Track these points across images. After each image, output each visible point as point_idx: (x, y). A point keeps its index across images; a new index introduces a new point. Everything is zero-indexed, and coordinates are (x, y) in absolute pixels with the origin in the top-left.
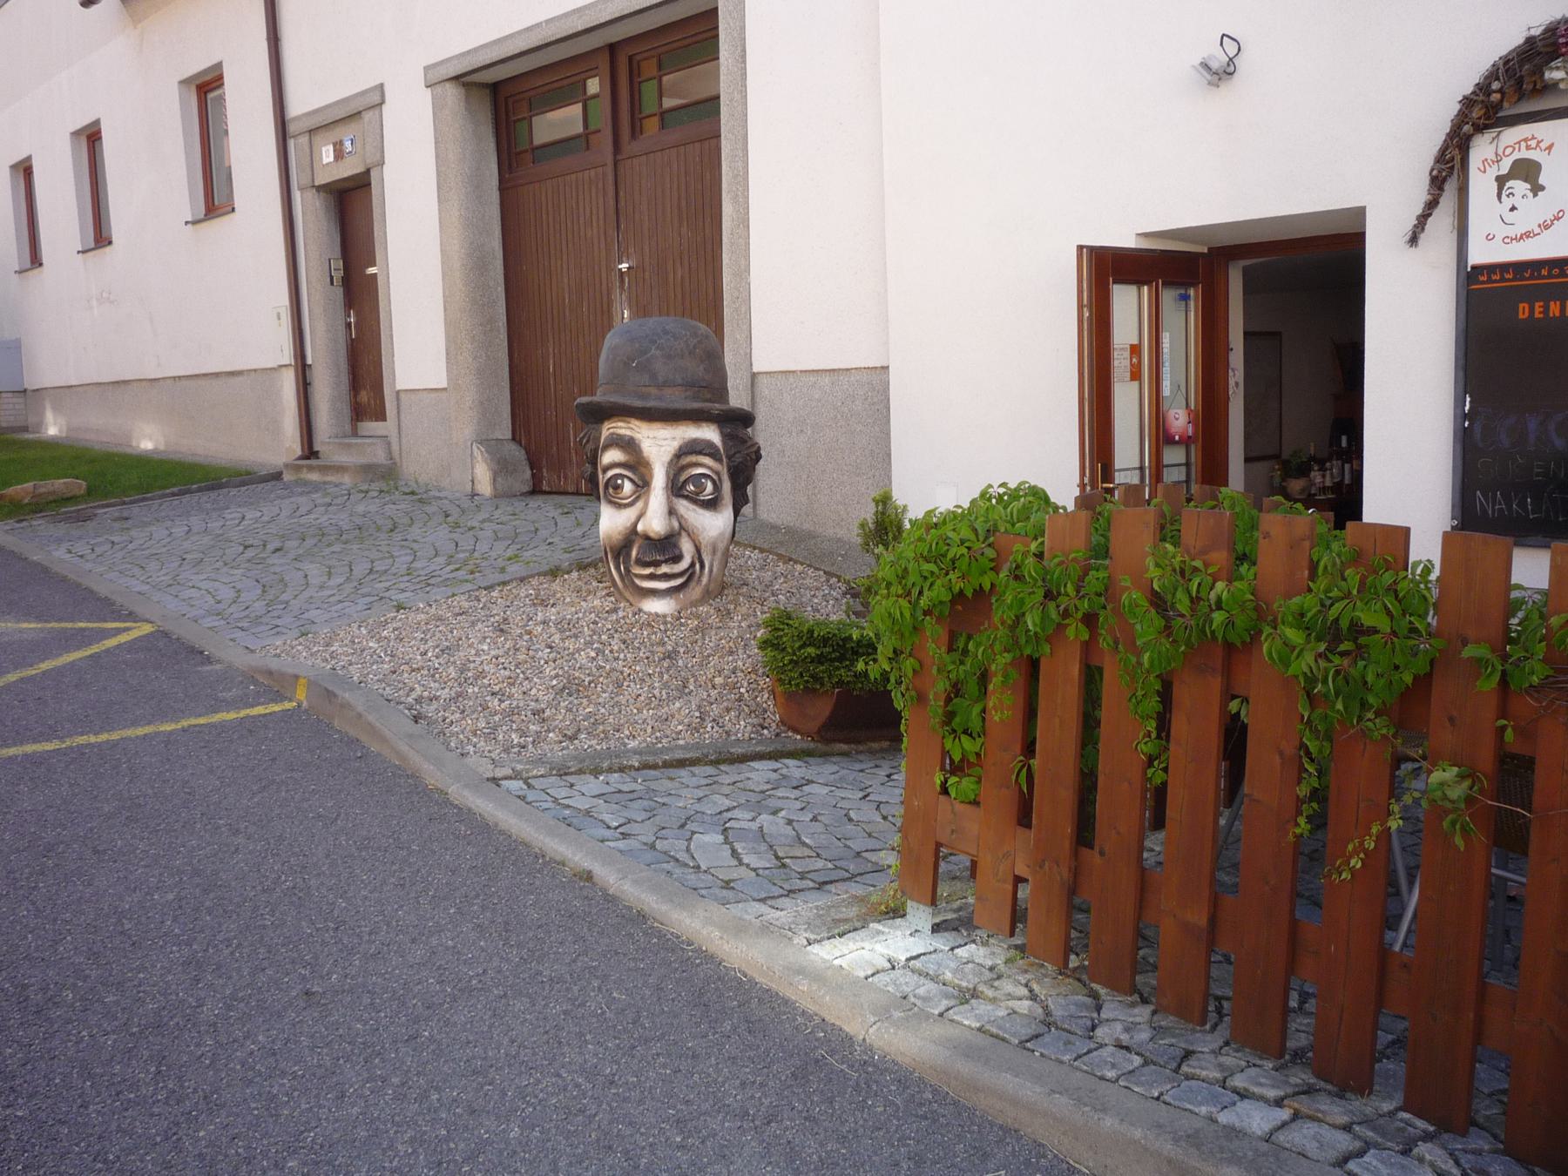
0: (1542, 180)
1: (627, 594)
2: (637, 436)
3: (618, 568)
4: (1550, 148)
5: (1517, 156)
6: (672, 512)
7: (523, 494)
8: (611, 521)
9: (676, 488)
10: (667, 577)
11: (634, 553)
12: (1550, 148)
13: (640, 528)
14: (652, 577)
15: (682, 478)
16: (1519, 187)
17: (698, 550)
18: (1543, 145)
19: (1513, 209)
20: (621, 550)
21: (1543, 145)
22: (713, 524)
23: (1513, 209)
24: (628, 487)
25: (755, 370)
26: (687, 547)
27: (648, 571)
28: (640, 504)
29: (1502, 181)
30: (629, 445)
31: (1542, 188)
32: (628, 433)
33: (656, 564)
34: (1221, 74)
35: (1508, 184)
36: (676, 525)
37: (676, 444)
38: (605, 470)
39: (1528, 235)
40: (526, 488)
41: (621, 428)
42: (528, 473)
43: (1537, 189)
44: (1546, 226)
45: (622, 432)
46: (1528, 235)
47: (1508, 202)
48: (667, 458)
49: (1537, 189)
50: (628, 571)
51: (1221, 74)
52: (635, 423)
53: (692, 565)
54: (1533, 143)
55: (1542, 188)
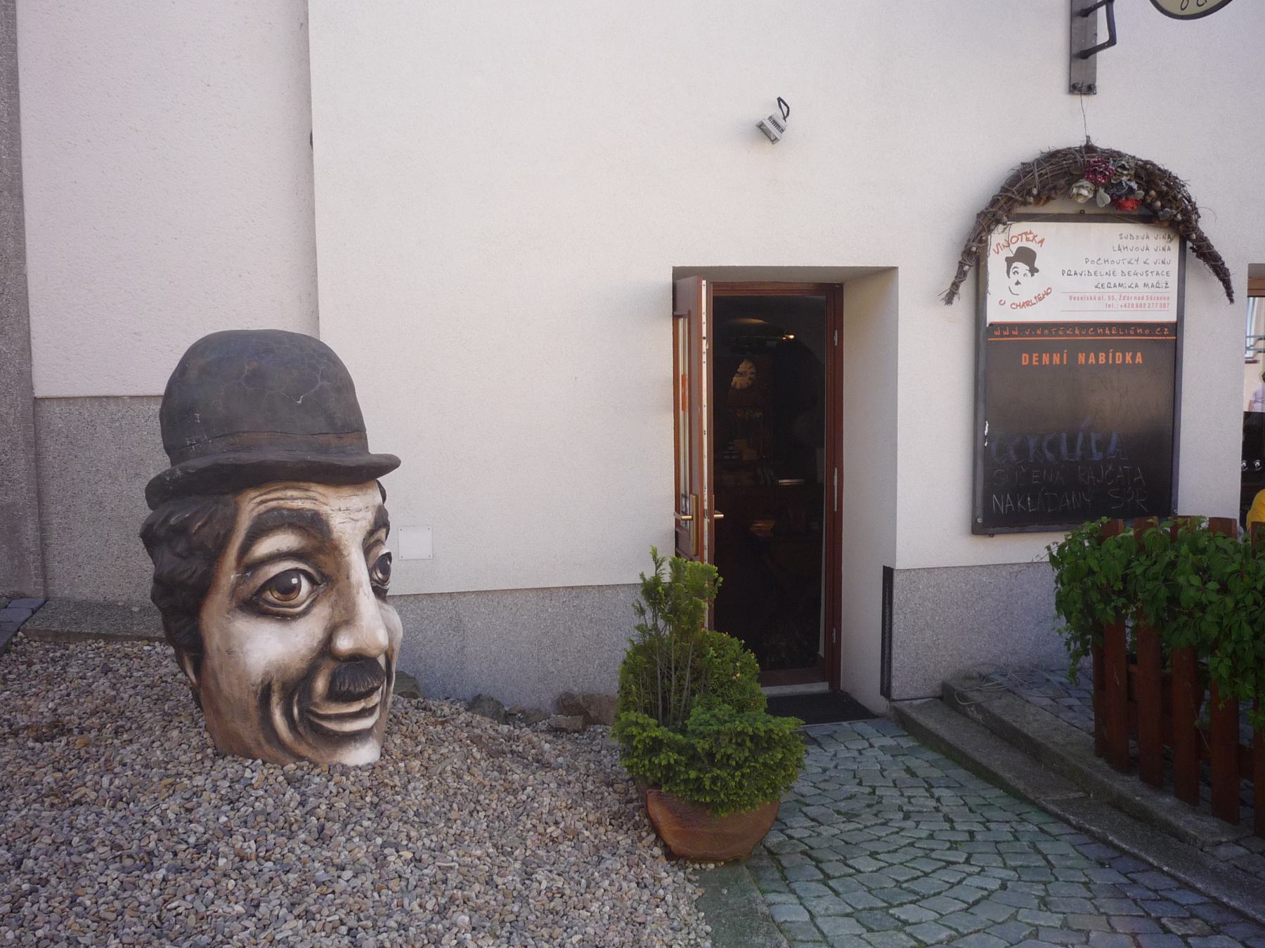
0: (1036, 265)
1: (303, 749)
2: (324, 509)
3: (288, 714)
4: (1042, 242)
5: (1020, 244)
11: (320, 685)
12: (1042, 242)
15: (372, 562)
16: (1022, 267)
18: (1038, 239)
19: (1018, 283)
20: (294, 687)
21: (1038, 239)
23: (1018, 283)
25: (39, 393)
27: (356, 707)
29: (1010, 261)
30: (313, 525)
31: (1037, 271)
32: (308, 505)
33: (368, 694)
34: (768, 132)
35: (1015, 264)
39: (1027, 304)
41: (296, 499)
43: (1033, 270)
44: (1040, 298)
45: (298, 504)
46: (1027, 304)
47: (1014, 278)
48: (360, 539)
49: (1033, 270)
51: (767, 132)
52: (318, 491)
54: (1031, 237)
55: (1037, 271)
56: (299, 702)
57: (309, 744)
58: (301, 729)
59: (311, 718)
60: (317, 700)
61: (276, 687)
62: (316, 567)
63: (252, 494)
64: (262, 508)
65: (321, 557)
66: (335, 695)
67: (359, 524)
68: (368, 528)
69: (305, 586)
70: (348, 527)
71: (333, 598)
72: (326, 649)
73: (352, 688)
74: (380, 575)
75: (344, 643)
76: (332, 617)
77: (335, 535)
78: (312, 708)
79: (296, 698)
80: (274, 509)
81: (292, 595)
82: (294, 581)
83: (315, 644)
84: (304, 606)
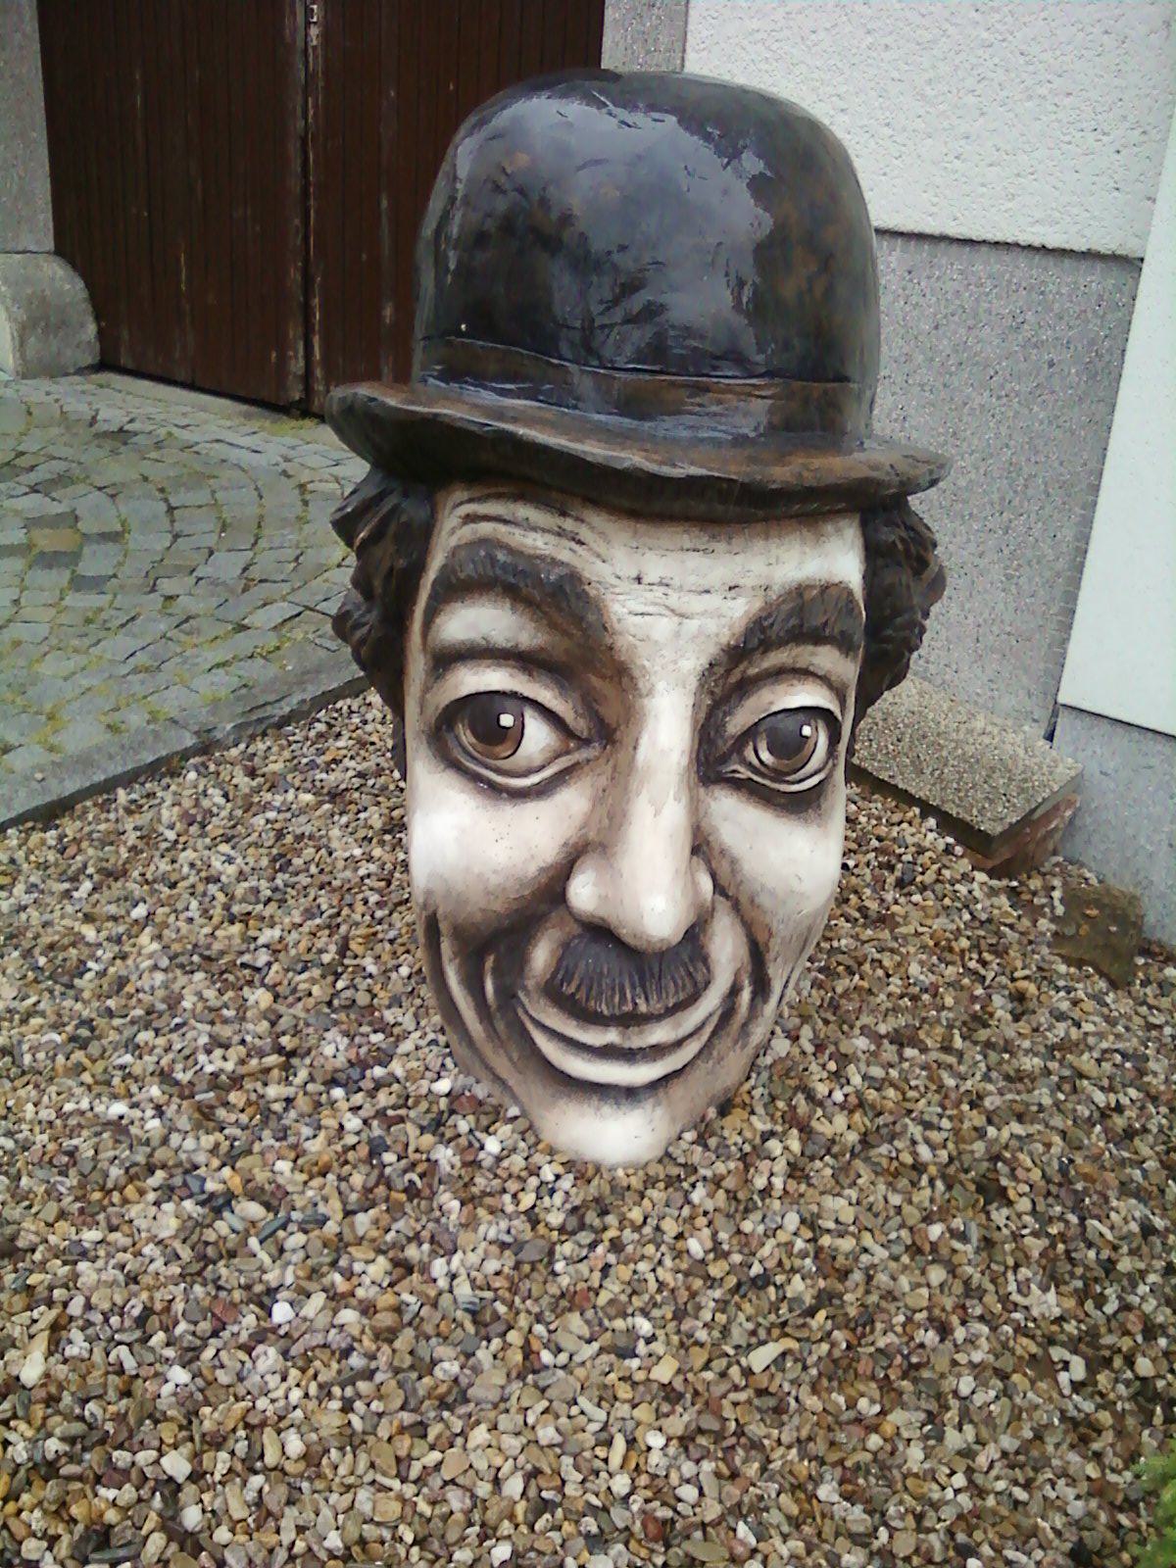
6: (701, 846)
7: (80, 371)
8: (463, 838)
9: (713, 761)
10: (657, 1051)
11: (541, 956)
13: (584, 893)
14: (608, 1053)
15: (738, 721)
17: (757, 955)
22: (798, 860)
24: (538, 737)
26: (726, 948)
28: (572, 804)
30: (561, 602)
33: (631, 1020)
36: (706, 884)
37: (739, 611)
38: (447, 659)
40: (88, 359)
41: (532, 533)
42: (91, 329)
50: (508, 996)
53: (735, 991)
56: (497, 971)
57: (511, 1059)
58: (500, 1026)
59: (520, 1011)
60: (530, 984)
61: (443, 927)
62: (589, 703)
63: (460, 495)
64: (468, 532)
65: (595, 681)
66: (553, 992)
67: (692, 625)
68: (726, 637)
69: (538, 737)
70: (662, 627)
71: (603, 781)
72: (550, 891)
73: (581, 996)
74: (765, 756)
75: (584, 893)
76: (585, 825)
77: (622, 642)
78: (521, 994)
79: (489, 963)
80: (483, 542)
81: (503, 750)
82: (507, 720)
83: (532, 870)
84: (535, 779)
